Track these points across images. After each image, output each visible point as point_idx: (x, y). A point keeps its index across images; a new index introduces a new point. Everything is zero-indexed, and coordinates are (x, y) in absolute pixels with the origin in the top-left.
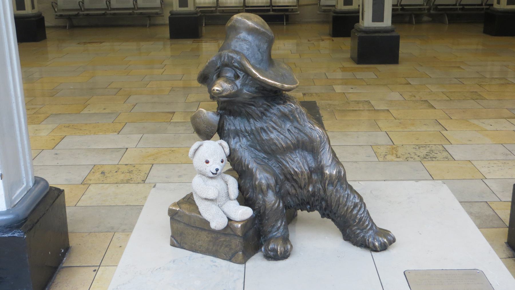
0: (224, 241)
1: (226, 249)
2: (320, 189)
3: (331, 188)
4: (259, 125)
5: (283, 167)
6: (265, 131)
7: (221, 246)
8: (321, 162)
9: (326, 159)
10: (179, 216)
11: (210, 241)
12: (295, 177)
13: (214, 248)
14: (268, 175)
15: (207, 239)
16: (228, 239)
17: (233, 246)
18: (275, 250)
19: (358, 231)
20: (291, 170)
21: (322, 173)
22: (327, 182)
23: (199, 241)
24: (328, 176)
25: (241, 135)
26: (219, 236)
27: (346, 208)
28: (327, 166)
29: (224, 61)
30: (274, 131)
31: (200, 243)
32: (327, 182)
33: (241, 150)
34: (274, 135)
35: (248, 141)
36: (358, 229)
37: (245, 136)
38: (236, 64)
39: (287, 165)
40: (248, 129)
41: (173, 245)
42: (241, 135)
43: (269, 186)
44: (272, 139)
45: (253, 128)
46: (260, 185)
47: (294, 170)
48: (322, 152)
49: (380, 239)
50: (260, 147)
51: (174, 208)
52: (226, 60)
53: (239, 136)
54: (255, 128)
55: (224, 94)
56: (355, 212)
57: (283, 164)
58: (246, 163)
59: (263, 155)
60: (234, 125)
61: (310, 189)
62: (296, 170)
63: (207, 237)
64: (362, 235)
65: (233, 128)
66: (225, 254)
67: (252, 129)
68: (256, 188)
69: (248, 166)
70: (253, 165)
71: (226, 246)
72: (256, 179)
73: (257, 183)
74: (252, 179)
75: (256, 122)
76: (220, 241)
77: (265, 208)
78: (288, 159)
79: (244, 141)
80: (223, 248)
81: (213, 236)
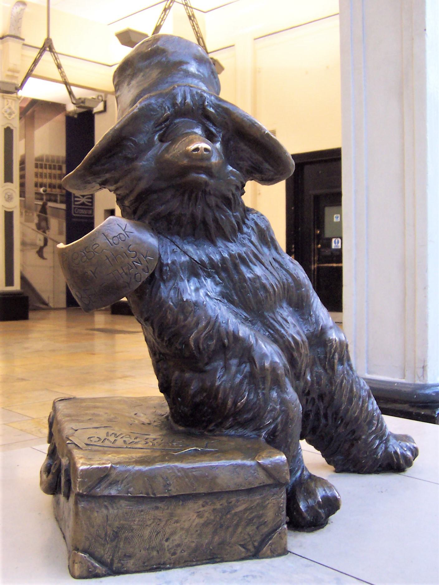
0: (246, 510)
1: (248, 529)
2: (320, 373)
3: (340, 368)
4: (234, 248)
5: (276, 336)
6: (244, 261)
7: (237, 525)
8: (317, 322)
10: (115, 483)
11: (206, 524)
12: (295, 354)
13: (217, 538)
15: (197, 521)
16: (257, 498)
17: (270, 515)
19: (377, 442)
20: (290, 339)
22: (337, 356)
23: (173, 533)
24: (338, 344)
25: (200, 272)
26: (233, 500)
27: (361, 403)
28: (331, 328)
30: (257, 263)
31: (176, 539)
32: (337, 356)
34: (258, 270)
35: (217, 284)
36: (376, 438)
37: (209, 276)
39: (283, 331)
40: (216, 258)
42: (200, 272)
44: (258, 277)
45: (226, 255)
46: (274, 367)
47: (293, 338)
49: (408, 444)
50: (237, 295)
52: (188, 100)
53: (197, 276)
54: (230, 255)
57: (277, 331)
59: (246, 315)
60: (185, 253)
62: (298, 338)
63: (200, 515)
64: (383, 446)
65: (184, 259)
66: (242, 546)
67: (223, 259)
68: (264, 378)
70: (244, 331)
71: (250, 522)
73: (267, 364)
74: (252, 361)
75: (229, 245)
76: (236, 514)
77: (288, 416)
78: (279, 318)
79: (209, 283)
80: (240, 530)
81: (218, 506)
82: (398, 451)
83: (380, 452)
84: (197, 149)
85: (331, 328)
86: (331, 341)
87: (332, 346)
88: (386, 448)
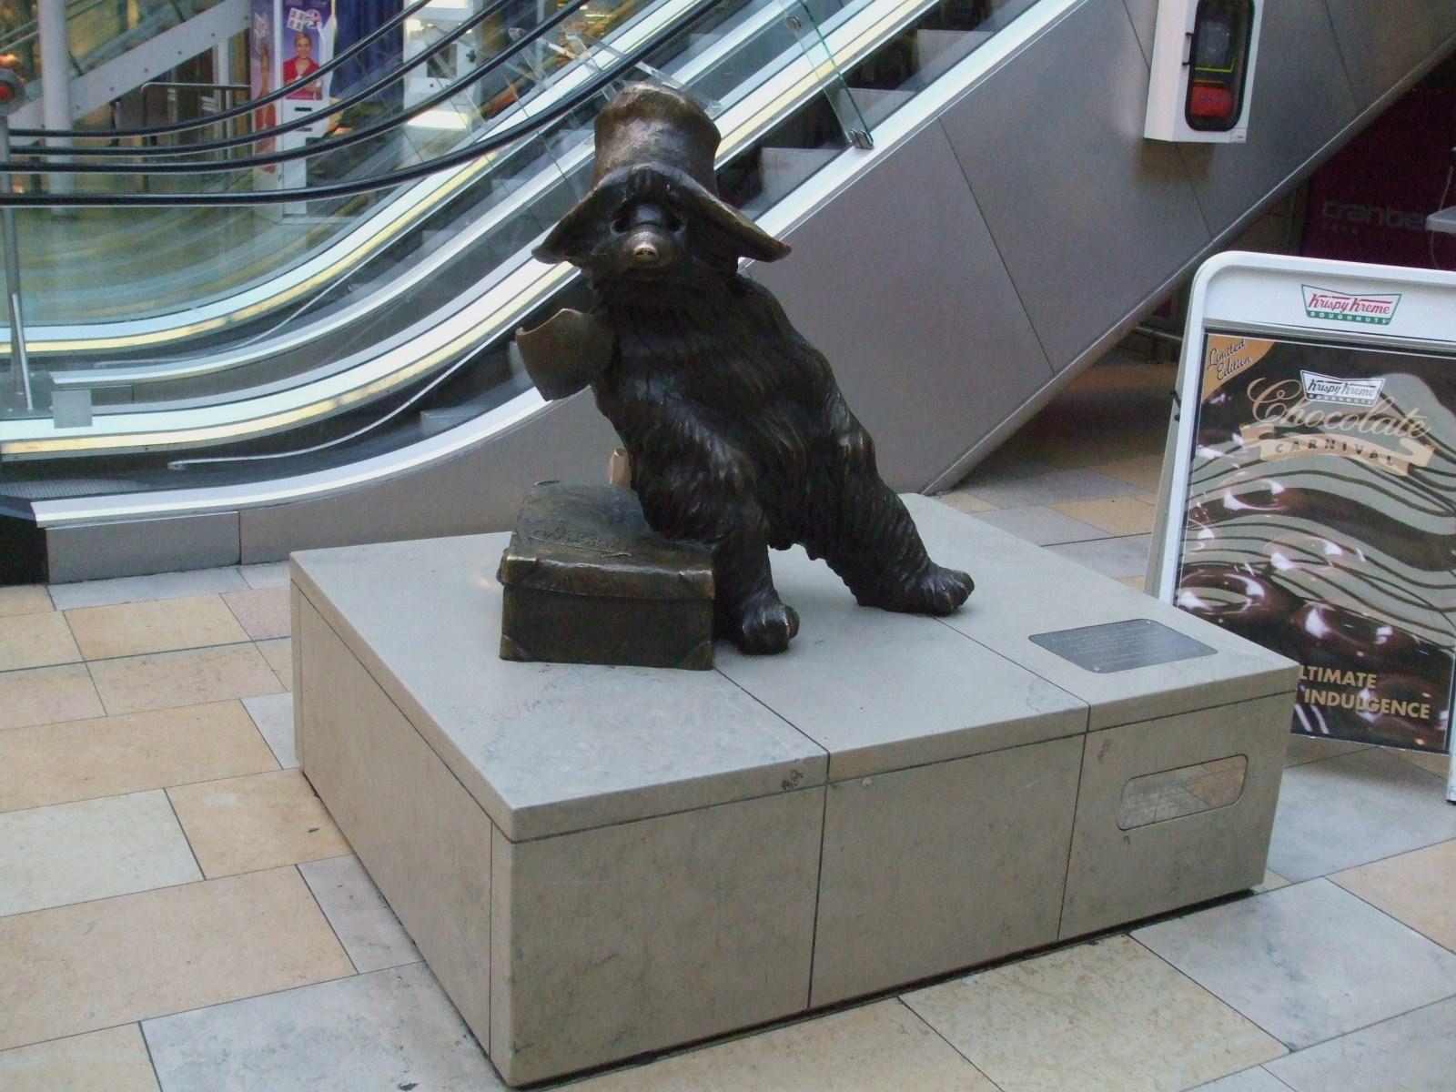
8: (829, 425)
9: (838, 418)
14: (740, 454)
18: (776, 627)
21: (836, 448)
22: (847, 469)
24: (850, 452)
29: (641, 188)
32: (847, 469)
33: (670, 401)
34: (738, 366)
38: (674, 193)
39: (767, 435)
41: (505, 657)
43: (748, 481)
47: (782, 445)
48: (830, 402)
51: (521, 558)
55: (662, 263)
56: (899, 531)
58: (687, 432)
61: (808, 489)
62: (786, 442)
64: (913, 581)
69: (691, 437)
70: (700, 433)
72: (718, 467)
73: (722, 474)
74: (707, 470)
82: (933, 588)
83: (907, 588)
84: (641, 252)
85: (845, 433)
86: (841, 448)
87: (842, 454)
88: (918, 583)
